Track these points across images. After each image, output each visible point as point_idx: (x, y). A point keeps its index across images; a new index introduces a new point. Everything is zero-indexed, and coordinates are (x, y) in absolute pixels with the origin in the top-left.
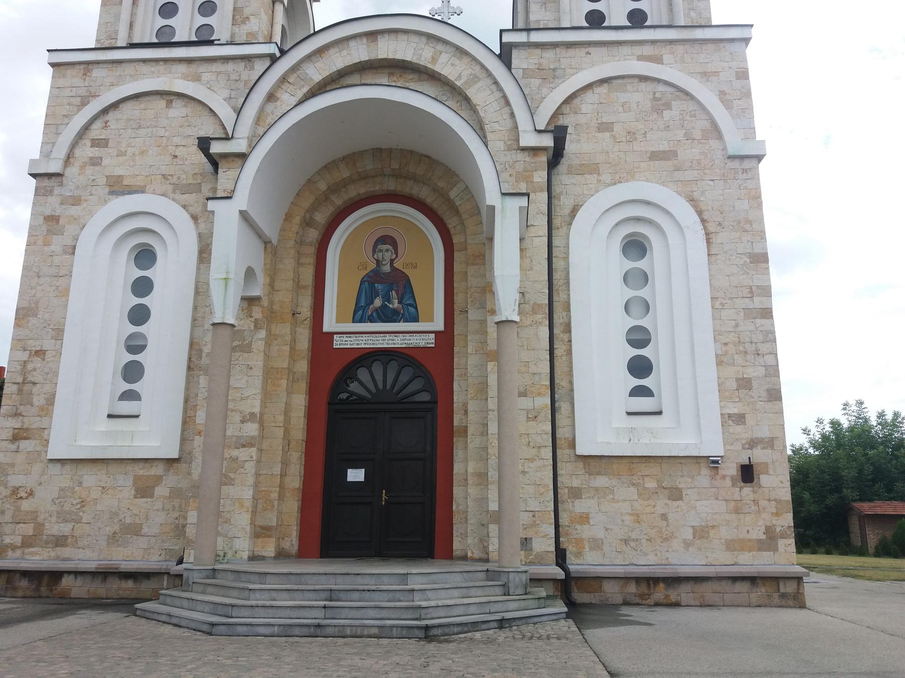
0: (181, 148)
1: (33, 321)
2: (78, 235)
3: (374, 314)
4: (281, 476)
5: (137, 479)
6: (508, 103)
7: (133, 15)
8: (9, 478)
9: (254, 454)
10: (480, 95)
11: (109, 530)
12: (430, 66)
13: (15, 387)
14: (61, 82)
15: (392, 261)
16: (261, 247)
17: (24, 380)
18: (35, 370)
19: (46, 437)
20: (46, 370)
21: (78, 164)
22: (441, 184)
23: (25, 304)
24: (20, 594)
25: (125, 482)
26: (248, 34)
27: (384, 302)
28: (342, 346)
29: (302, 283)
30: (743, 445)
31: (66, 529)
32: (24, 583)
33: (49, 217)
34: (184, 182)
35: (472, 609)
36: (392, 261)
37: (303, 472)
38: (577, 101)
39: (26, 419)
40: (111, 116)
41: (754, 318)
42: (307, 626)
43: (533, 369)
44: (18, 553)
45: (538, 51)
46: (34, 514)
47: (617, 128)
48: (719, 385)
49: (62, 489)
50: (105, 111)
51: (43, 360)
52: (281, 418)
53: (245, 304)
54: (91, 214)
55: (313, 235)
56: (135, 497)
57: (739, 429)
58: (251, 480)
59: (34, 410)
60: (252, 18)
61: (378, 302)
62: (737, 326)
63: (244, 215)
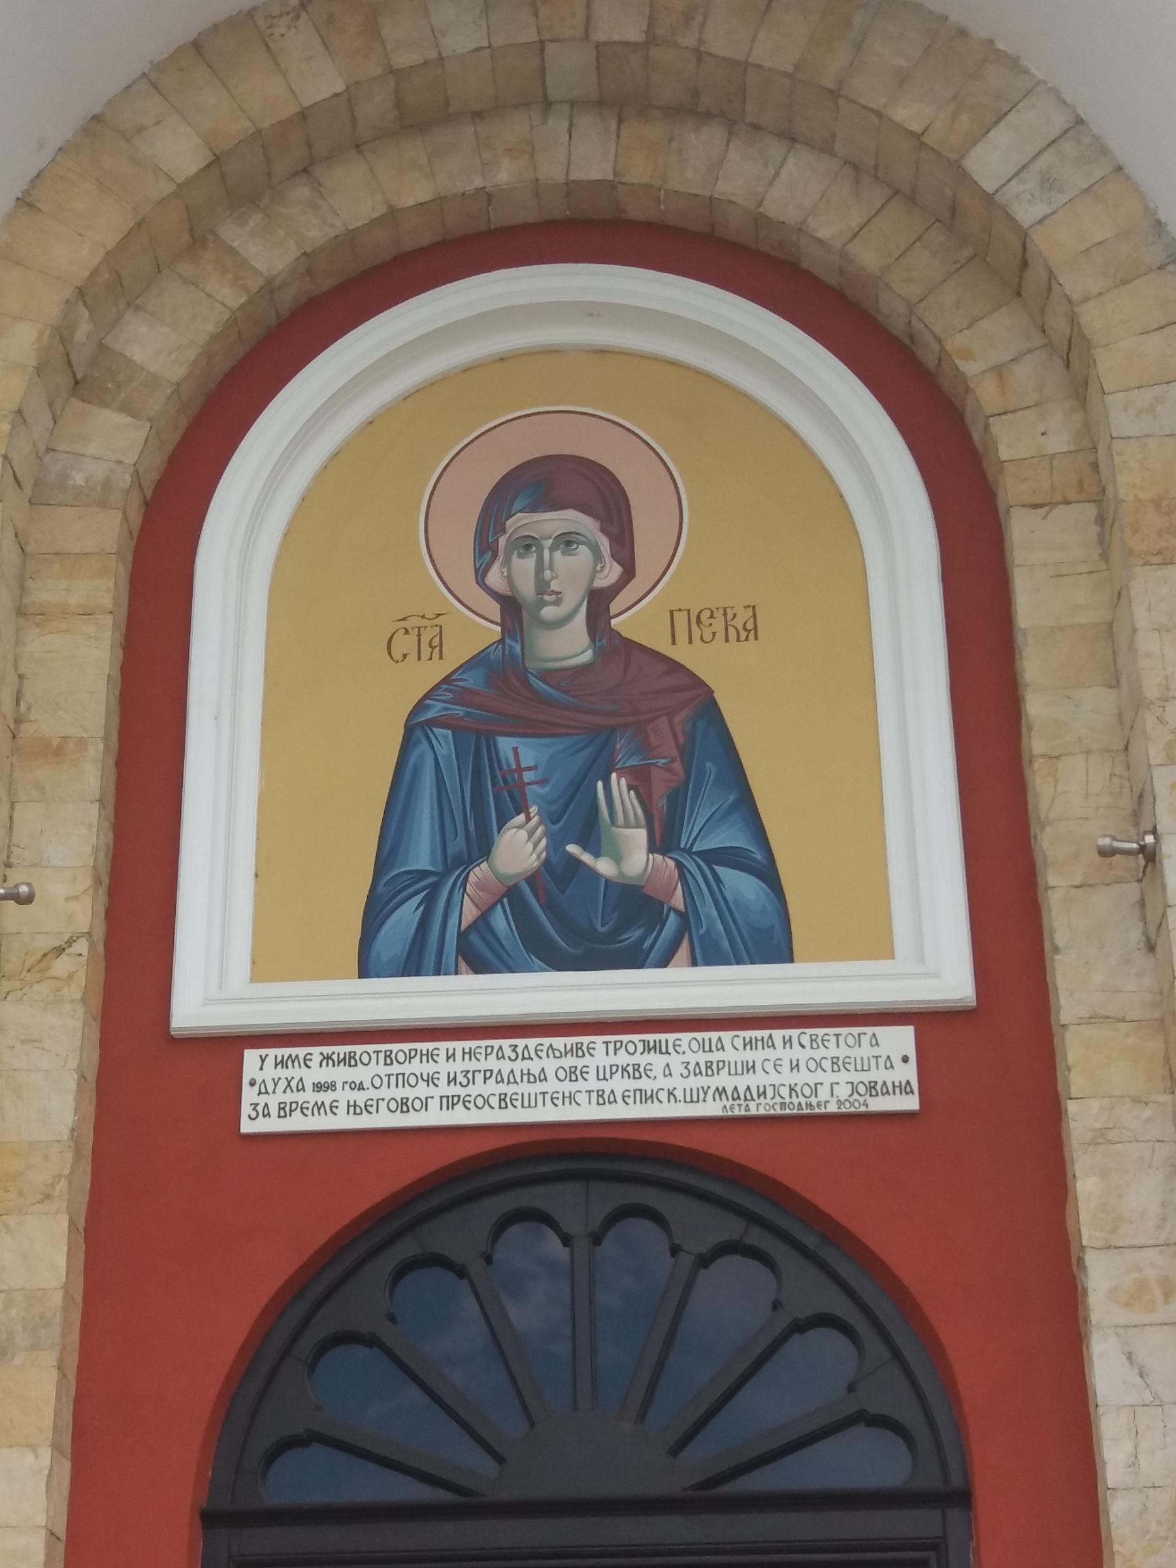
3: (500, 921)
15: (598, 603)
27: (556, 843)
28: (297, 1123)
29: (45, 725)
36: (598, 603)
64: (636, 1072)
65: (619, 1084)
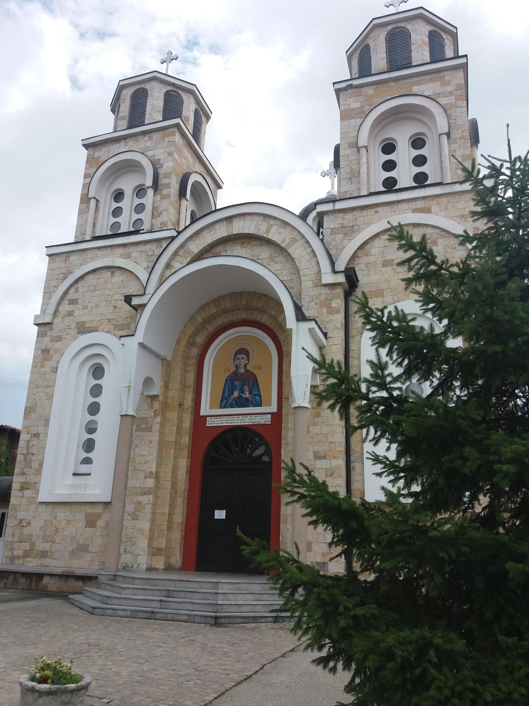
0: (119, 302)
1: (33, 415)
2: (59, 360)
4: (169, 514)
5: (87, 515)
6: (315, 255)
7: (95, 218)
8: (18, 513)
9: (151, 499)
10: (297, 251)
11: (70, 548)
12: (265, 235)
13: (23, 456)
14: (53, 266)
15: (245, 365)
16: (159, 363)
17: (27, 452)
18: (33, 446)
19: (38, 488)
20: (40, 446)
21: (61, 316)
22: (273, 313)
23: (30, 405)
24: (20, 587)
25: (80, 517)
26: (161, 224)
27: (240, 393)
28: (212, 425)
29: (188, 384)
31: (46, 546)
32: (23, 580)
33: (44, 349)
34: (120, 323)
35: (258, 608)
36: (245, 365)
37: (185, 512)
38: (368, 247)
39: (28, 477)
40: (80, 284)
42: (146, 612)
43: (330, 439)
44: (21, 561)
45: (341, 215)
46: (30, 536)
49: (45, 521)
50: (76, 281)
51: (38, 439)
52: (170, 475)
53: (149, 400)
54: (67, 346)
55: (195, 351)
56: (86, 527)
58: (149, 517)
59: (32, 471)
60: (164, 213)
61: (236, 394)
63: (141, 345)
64: (244, 420)
65: (242, 421)
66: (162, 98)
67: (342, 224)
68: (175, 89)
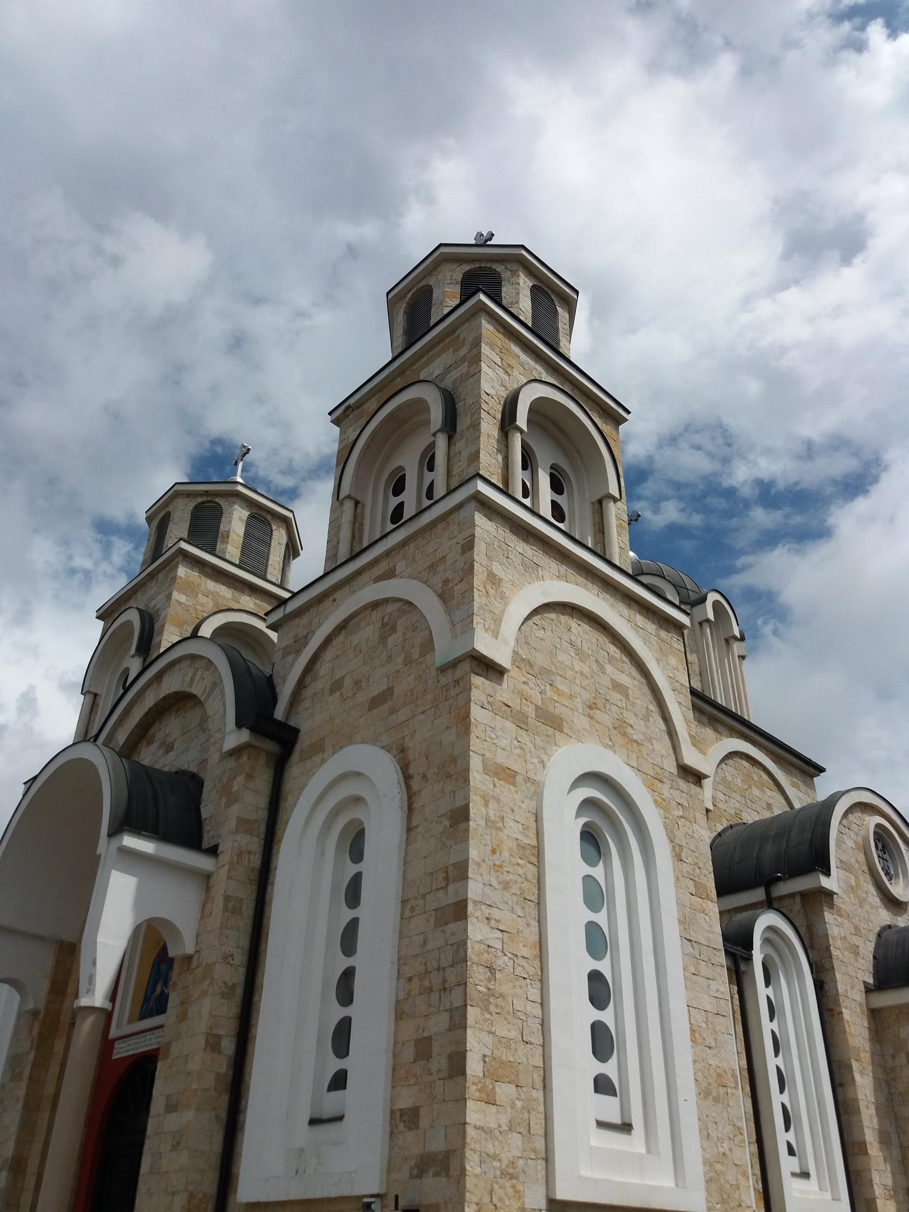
12: (188, 690)
30: (412, 1169)
41: (446, 924)
47: (347, 683)
48: (395, 1056)
57: (410, 1136)
61: (159, 987)
62: (425, 943)
66: (188, 516)
67: (296, 635)
68: (209, 499)
